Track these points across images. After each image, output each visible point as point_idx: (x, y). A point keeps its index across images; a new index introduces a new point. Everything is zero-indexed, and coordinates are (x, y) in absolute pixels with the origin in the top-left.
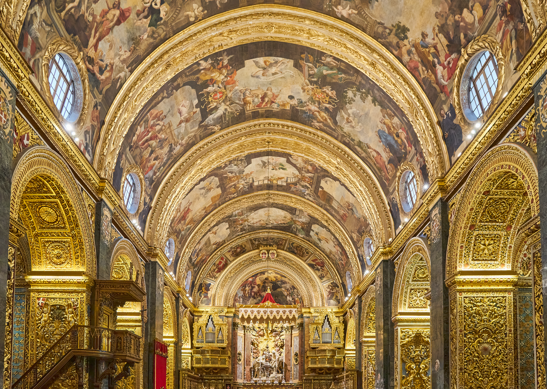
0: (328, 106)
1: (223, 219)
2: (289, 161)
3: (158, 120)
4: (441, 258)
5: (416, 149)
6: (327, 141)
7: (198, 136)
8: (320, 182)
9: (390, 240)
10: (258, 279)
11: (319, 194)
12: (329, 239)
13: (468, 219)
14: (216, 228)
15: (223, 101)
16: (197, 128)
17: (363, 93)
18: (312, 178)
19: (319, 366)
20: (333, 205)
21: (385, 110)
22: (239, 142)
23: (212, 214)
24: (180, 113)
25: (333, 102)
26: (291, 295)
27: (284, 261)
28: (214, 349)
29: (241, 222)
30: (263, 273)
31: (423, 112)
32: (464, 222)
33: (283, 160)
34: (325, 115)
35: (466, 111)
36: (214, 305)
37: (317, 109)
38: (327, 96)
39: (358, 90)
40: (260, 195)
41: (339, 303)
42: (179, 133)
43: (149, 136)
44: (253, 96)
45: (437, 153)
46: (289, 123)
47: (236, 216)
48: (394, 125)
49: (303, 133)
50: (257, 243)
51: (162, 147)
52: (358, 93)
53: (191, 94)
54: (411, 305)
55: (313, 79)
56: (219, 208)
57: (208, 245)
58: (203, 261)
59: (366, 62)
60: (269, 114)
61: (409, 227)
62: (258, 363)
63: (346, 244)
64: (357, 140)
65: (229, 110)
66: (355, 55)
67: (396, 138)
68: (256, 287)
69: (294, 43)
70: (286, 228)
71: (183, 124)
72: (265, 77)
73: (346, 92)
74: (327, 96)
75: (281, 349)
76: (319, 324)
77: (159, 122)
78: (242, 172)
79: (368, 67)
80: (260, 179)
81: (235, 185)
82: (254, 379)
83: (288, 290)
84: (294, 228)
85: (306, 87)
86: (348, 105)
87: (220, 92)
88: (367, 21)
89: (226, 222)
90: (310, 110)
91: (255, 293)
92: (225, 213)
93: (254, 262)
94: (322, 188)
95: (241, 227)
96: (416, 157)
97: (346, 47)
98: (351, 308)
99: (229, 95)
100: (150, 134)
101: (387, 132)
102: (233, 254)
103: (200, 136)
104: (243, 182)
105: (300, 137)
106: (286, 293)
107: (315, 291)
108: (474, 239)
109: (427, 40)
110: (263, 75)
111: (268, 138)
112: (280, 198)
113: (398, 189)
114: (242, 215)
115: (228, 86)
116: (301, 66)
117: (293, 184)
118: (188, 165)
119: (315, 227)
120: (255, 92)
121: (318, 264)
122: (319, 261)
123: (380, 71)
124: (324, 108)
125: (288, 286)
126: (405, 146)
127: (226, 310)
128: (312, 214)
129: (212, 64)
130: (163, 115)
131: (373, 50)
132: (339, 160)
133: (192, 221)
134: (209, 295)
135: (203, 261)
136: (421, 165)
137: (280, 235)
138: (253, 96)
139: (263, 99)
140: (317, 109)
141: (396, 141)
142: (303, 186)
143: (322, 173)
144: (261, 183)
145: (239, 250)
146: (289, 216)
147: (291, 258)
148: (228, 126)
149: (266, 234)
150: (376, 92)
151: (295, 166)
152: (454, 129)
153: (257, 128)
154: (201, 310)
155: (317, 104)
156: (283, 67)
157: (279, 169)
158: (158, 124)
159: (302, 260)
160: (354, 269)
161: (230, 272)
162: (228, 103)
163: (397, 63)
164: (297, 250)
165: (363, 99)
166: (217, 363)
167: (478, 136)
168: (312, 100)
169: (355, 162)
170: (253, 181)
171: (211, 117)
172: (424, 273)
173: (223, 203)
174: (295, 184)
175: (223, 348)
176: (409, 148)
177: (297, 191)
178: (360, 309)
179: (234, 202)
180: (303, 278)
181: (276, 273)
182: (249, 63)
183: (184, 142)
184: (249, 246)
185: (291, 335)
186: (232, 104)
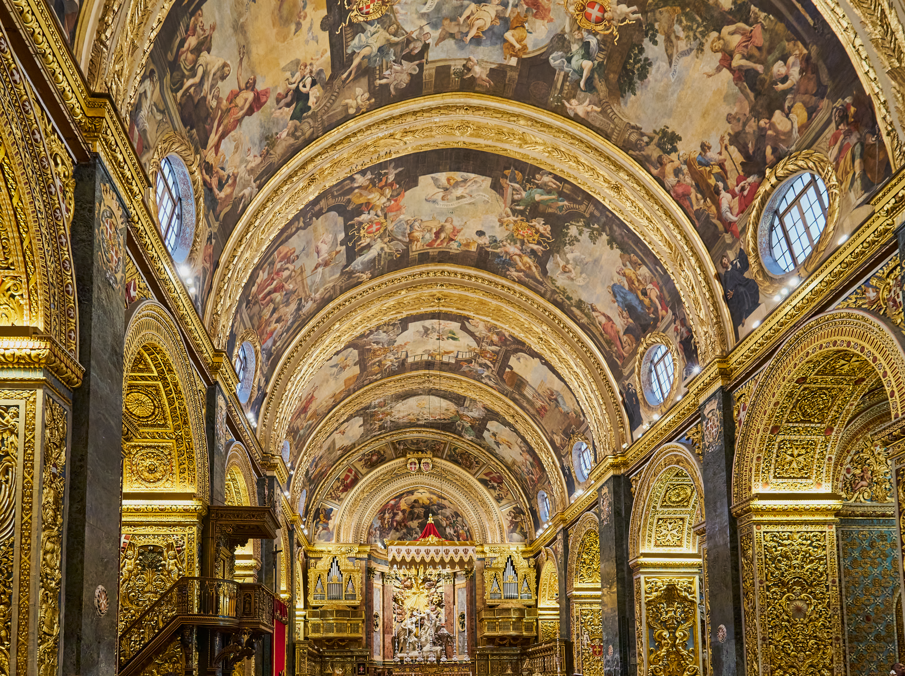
0: (535, 247)
2: (464, 328)
3: (288, 262)
4: (724, 473)
5: (674, 314)
6: (528, 298)
8: (508, 359)
9: (625, 446)
10: (403, 501)
11: (504, 377)
12: (513, 442)
13: (769, 418)
14: (346, 424)
15: (380, 237)
16: (338, 275)
17: (594, 229)
18: (496, 353)
19: (500, 633)
20: (525, 393)
21: (627, 256)
23: (342, 404)
24: (318, 253)
25: (545, 242)
26: (452, 525)
27: (442, 475)
28: (341, 608)
29: (381, 416)
30: (411, 493)
31: (693, 260)
32: (764, 422)
33: (455, 326)
34: (529, 260)
35: (766, 261)
36: (338, 541)
37: (518, 252)
38: (536, 233)
39: (587, 225)
40: (414, 377)
41: (526, 538)
42: (313, 283)
43: (272, 286)
44: (423, 230)
45: (715, 320)
46: (473, 272)
48: (640, 278)
49: (492, 287)
50: (402, 447)
51: (287, 303)
52: (586, 230)
53: (336, 224)
54: (658, 542)
55: (518, 208)
58: (322, 475)
59: (606, 185)
60: (444, 257)
61: (659, 428)
62: (404, 629)
63: (541, 450)
64: (575, 298)
66: (591, 173)
67: (641, 297)
68: (400, 513)
69: (496, 153)
70: (447, 426)
71: (320, 270)
72: (445, 203)
73: (568, 228)
74: (536, 233)
75: (438, 608)
76: (498, 569)
77: (288, 265)
78: (392, 342)
79: (607, 191)
80: (417, 354)
81: (380, 361)
82: (399, 655)
83: (447, 518)
85: (506, 219)
86: (568, 246)
87: (377, 224)
88: (614, 123)
89: (360, 415)
90: (507, 253)
91: (399, 523)
92: (361, 403)
93: (398, 476)
94: (511, 368)
96: (673, 326)
97: (578, 162)
98: (548, 545)
99: (390, 228)
100: (275, 283)
101: (627, 287)
103: (341, 287)
104: (392, 358)
105: (487, 292)
107: (491, 519)
108: (776, 446)
109: (709, 154)
110: (443, 199)
111: (439, 292)
113: (639, 371)
114: (384, 406)
115: (390, 214)
116: (502, 188)
117: (465, 361)
118: (321, 331)
119: (493, 426)
120: (428, 224)
122: (494, 475)
123: (628, 199)
124: (529, 250)
125: (448, 512)
126: (656, 309)
127: (357, 549)
128: (491, 406)
129: (372, 181)
130: (295, 254)
131: (619, 167)
132: (545, 328)
133: (315, 414)
134: (330, 526)
135: (322, 475)
136: (681, 337)
137: (437, 436)
138: (423, 230)
139: (437, 234)
140: (518, 252)
141: (641, 302)
142: (480, 365)
143: (513, 347)
144: (418, 359)
145: (375, 458)
146: (453, 407)
148: (382, 274)
149: (416, 434)
150: (615, 228)
151: (472, 334)
152: (744, 286)
153: (424, 277)
154: (317, 548)
155: (518, 245)
156: (475, 187)
157: (448, 338)
158: (287, 269)
160: (555, 487)
161: (363, 491)
162: (387, 240)
163: (656, 187)
165: (593, 239)
166: (345, 631)
167: (791, 298)
168: (513, 239)
169: (570, 330)
171: (359, 259)
172: (679, 496)
173: (359, 389)
174: (469, 361)
175: (355, 607)
176: (662, 312)
178: (566, 546)
179: (375, 387)
180: (471, 501)
181: (431, 493)
182: (425, 180)
183: (318, 296)
184: (390, 452)
185: (454, 585)
186: (392, 240)
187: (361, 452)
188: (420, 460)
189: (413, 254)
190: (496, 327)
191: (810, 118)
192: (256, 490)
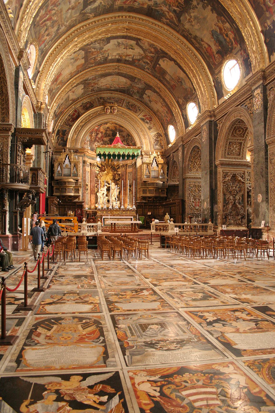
0: (176, 8)
1: (82, 82)
2: (137, 44)
7: (78, 22)
10: (102, 128)
11: (156, 69)
18: (153, 57)
20: (166, 77)
25: (180, 6)
29: (93, 85)
30: (106, 123)
33: (133, 43)
34: (172, 15)
37: (167, 10)
40: (111, 66)
46: (144, 18)
47: (90, 80)
52: (201, 3)
65: (103, 3)
78: (101, 48)
80: (114, 54)
81: (95, 58)
84: (131, 91)
86: (191, 10)
90: (162, 10)
91: (99, 138)
92: (84, 78)
93: (100, 115)
94: (160, 65)
95: (92, 88)
102: (84, 108)
104: (101, 56)
111: (128, 26)
114: (95, 79)
117: (137, 60)
122: (148, 116)
124: (172, 10)
128: (148, 83)
140: (167, 10)
142: (144, 63)
143: (162, 55)
144: (113, 57)
145: (88, 105)
146: (129, 82)
147: (128, 114)
148: (100, 15)
151: (141, 47)
155: (168, 7)
157: (129, 48)
159: (135, 115)
164: (132, 107)
170: (108, 56)
173: (83, 71)
174: (139, 60)
177: (139, 65)
179: (91, 70)
187: (82, 102)
188: (111, 107)
189: (116, 7)
190: (154, 45)
192: (33, 120)
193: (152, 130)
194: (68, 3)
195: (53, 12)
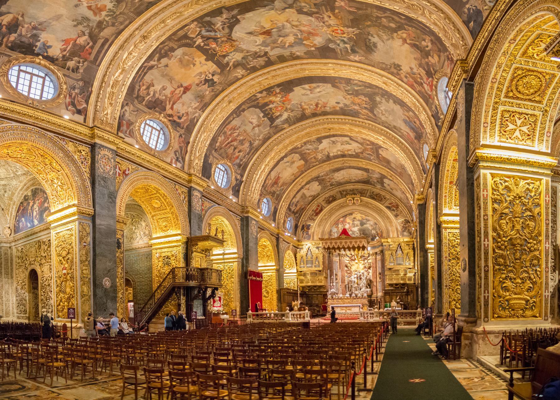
2: (351, 139)
15: (286, 110)
18: (372, 149)
22: (305, 131)
26: (374, 229)
27: (366, 205)
30: (351, 214)
36: (313, 240)
56: (306, 173)
57: (304, 197)
60: (325, 113)
99: (289, 107)
105: (351, 124)
106: (370, 228)
112: (354, 162)
121: (394, 206)
134: (310, 233)
142: (368, 154)
151: (357, 142)
153: (318, 122)
161: (325, 215)
186: (292, 111)
191: (439, 59)
193: (399, 217)
194: (251, 124)
195: (235, 134)
